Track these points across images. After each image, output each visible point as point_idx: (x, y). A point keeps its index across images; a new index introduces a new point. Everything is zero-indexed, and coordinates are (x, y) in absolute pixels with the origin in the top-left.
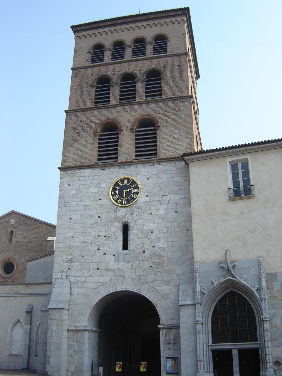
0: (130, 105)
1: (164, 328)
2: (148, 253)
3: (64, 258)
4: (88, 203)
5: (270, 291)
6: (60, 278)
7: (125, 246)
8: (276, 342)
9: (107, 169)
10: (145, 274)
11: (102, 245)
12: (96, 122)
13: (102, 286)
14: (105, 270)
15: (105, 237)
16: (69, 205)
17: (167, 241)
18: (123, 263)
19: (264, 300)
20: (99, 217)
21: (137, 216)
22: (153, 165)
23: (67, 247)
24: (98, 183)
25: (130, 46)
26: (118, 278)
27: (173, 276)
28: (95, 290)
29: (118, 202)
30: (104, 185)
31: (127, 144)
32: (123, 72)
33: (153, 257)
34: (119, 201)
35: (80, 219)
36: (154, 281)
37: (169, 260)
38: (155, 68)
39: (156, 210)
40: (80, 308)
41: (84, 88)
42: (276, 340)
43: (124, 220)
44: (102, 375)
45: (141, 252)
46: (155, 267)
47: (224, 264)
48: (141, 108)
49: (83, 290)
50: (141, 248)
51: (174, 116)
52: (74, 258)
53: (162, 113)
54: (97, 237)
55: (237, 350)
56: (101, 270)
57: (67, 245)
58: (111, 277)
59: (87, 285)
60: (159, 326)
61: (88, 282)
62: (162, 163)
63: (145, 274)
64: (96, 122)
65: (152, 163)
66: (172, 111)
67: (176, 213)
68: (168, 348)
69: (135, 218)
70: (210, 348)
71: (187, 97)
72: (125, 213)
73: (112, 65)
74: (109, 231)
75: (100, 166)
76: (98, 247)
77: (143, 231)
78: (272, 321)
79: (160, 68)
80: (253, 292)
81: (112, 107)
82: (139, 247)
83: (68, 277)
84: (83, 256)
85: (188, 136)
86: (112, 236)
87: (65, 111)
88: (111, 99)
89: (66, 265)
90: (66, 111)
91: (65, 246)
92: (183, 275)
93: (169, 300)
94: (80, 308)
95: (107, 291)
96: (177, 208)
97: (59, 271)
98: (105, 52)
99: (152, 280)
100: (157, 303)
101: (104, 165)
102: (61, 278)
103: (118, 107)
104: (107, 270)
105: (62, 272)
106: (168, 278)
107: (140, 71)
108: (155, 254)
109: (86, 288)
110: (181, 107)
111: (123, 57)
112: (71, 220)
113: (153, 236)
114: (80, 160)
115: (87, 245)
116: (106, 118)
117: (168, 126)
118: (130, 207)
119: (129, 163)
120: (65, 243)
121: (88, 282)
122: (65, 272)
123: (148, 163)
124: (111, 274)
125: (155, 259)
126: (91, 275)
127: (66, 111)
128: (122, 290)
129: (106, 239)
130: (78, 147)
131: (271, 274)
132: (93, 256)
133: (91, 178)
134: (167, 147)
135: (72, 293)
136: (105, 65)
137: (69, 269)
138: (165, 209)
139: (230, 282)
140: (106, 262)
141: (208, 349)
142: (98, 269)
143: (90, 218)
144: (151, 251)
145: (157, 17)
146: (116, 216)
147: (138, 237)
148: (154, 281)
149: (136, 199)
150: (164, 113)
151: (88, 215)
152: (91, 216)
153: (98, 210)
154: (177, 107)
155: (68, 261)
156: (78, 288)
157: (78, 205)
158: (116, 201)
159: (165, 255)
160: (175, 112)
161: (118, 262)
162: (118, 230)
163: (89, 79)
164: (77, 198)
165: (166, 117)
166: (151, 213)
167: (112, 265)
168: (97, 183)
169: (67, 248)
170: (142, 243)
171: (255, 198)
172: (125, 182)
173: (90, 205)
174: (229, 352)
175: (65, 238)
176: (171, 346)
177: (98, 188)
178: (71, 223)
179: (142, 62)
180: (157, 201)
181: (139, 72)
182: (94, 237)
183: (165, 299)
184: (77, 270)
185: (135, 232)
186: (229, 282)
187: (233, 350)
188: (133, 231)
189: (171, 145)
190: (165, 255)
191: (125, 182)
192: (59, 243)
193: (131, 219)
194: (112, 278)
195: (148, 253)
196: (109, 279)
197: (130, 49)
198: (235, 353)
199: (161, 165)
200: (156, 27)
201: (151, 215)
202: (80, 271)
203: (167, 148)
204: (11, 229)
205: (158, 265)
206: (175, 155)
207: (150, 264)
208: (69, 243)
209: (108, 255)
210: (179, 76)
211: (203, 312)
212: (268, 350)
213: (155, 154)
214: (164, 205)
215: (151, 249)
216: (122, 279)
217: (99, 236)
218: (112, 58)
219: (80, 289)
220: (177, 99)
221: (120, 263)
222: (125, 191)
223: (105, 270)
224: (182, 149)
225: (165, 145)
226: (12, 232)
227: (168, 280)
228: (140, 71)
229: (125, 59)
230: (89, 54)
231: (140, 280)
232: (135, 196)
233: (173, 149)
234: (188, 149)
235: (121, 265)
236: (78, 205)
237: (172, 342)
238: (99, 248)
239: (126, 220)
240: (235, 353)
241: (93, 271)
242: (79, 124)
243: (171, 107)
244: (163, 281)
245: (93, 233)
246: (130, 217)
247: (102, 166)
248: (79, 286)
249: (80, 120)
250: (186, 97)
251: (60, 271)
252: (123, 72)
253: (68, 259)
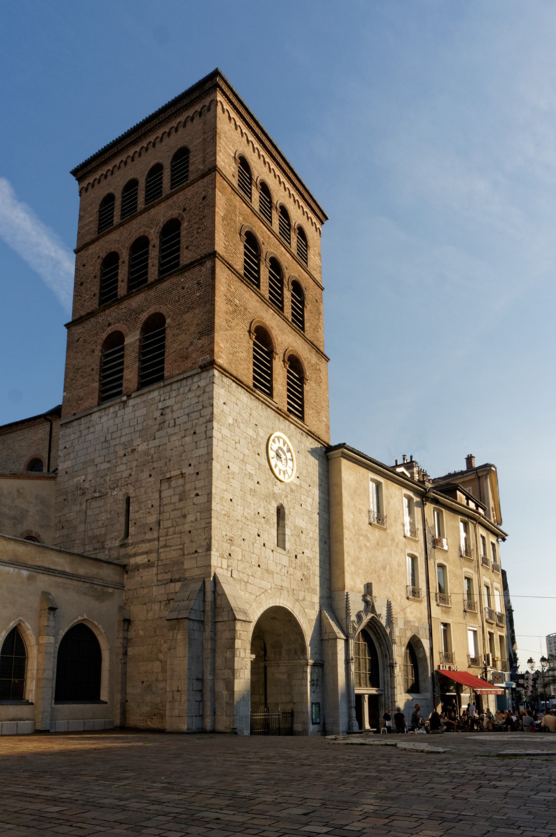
3: (224, 533)
16: (226, 442)
91: (223, 512)
102: (221, 568)
169: (226, 518)
178: (230, 476)
236: (236, 448)
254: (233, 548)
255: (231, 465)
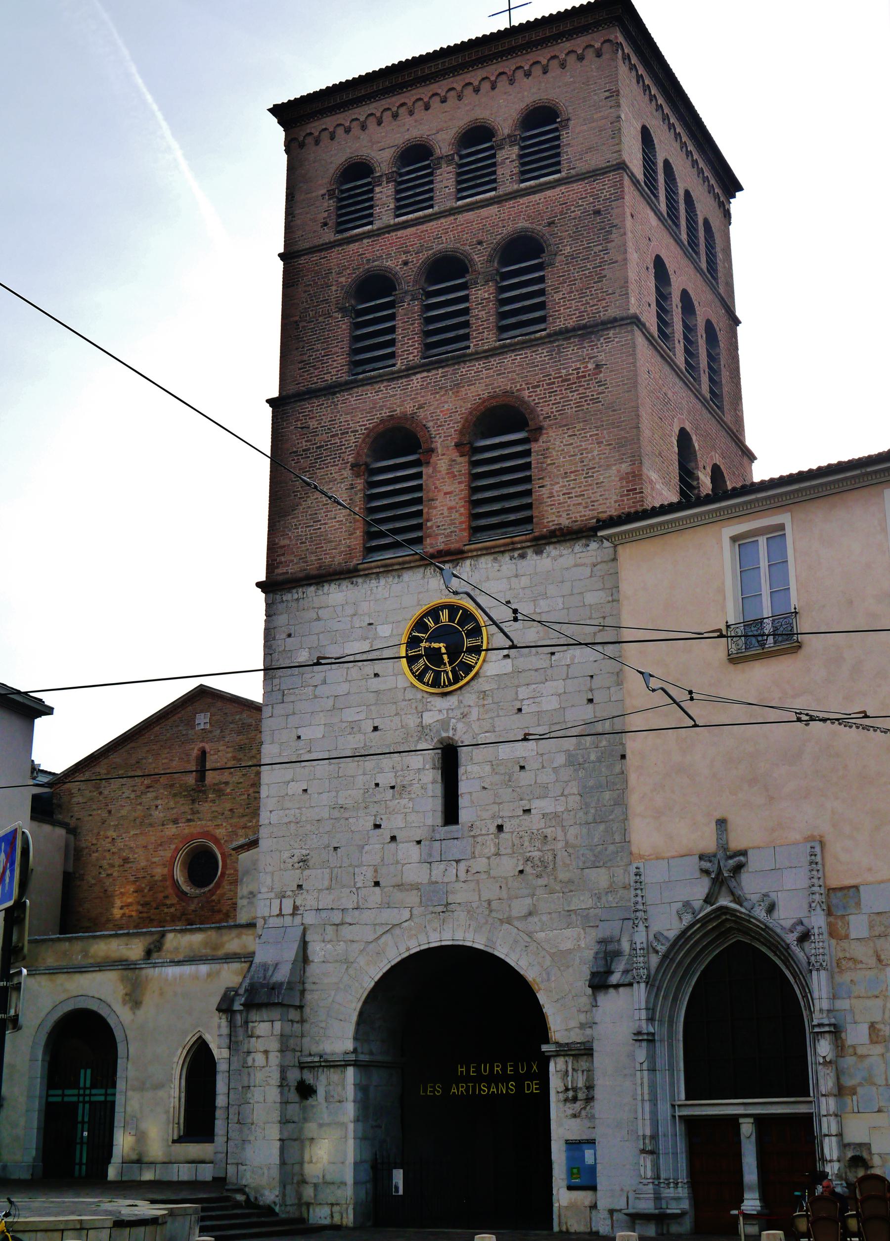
0: (454, 364)
1: (557, 1054)
2: (512, 833)
3: (286, 855)
4: (344, 688)
5: (840, 942)
6: (278, 915)
7: (451, 815)
8: (855, 1098)
9: (394, 577)
10: (504, 894)
11: (386, 813)
12: (357, 431)
13: (388, 935)
14: (394, 886)
15: (393, 787)
16: (292, 698)
17: (565, 793)
18: (442, 866)
19: (818, 970)
20: (376, 729)
21: (479, 719)
22: (523, 556)
23: (292, 824)
24: (370, 624)
25: (449, 159)
26: (431, 909)
27: (582, 898)
28: (372, 946)
29: (426, 680)
30: (384, 630)
31: (446, 494)
32: (430, 252)
33: (526, 844)
34: (430, 676)
35: (324, 736)
36: (530, 914)
37: (570, 850)
38: (526, 230)
39: (532, 701)
40: (330, 1000)
41: (321, 319)
42: (855, 1093)
43: (444, 735)
44: (401, 1192)
45: (493, 829)
46: (532, 874)
47: (710, 861)
48: (484, 372)
49: (338, 948)
50: (493, 817)
51: (581, 390)
52: (311, 853)
53: (548, 384)
54: (371, 790)
55: (751, 1120)
56: (385, 887)
57: (292, 818)
58: (412, 908)
59: (346, 931)
60: (544, 1048)
61: (350, 924)
62: (550, 548)
63: (504, 894)
64: (358, 428)
65: (520, 552)
66: (578, 373)
67: (590, 706)
68: (570, 1112)
69: (473, 726)
70: (677, 1114)
71: (622, 323)
72: (445, 712)
73: (399, 233)
74: (402, 770)
75: (370, 572)
76: (375, 820)
77: (498, 765)
78: (843, 1035)
79: (540, 228)
80: (788, 945)
81: (401, 377)
82: (486, 815)
83: (299, 912)
84: (335, 849)
85: (624, 454)
86: (411, 785)
87: (268, 401)
88: (398, 349)
89: (291, 878)
90: (270, 402)
91: (286, 820)
92: (609, 895)
93: (571, 970)
94: (333, 1001)
95: (402, 949)
96: (591, 690)
97: (272, 895)
98: (377, 189)
99: (524, 912)
100: (538, 980)
101: (383, 566)
102: (280, 915)
103: (419, 376)
104: (400, 886)
105: (282, 896)
106: (569, 906)
107: (480, 243)
108: (533, 833)
109: (344, 941)
110: (602, 357)
111: (429, 202)
112: (301, 743)
113: (525, 778)
114: (316, 556)
115: (347, 815)
116: (385, 413)
117: (565, 426)
118: (459, 692)
119: (455, 556)
120: (287, 812)
121: (350, 924)
122: (289, 896)
123: (509, 550)
124: (413, 898)
125: (532, 849)
126: (358, 902)
127: (270, 402)
128: (444, 943)
129: (397, 796)
130: (310, 515)
131: (841, 889)
132: (363, 848)
133: (349, 610)
134: (564, 494)
135: (311, 959)
136: (378, 235)
137: (300, 887)
138: (559, 695)
139: (728, 917)
140: (398, 862)
141: (674, 1117)
142: (377, 884)
143: (350, 734)
144: (519, 826)
145: (527, 43)
146: (422, 722)
147: (483, 785)
148: (530, 914)
149: (474, 667)
150: (554, 383)
151: (345, 725)
152: (354, 727)
153: (373, 708)
154: (591, 358)
155: (297, 865)
156: (324, 941)
157: (316, 697)
158: (420, 677)
159: (560, 835)
160: (584, 376)
161: (430, 863)
162: (427, 767)
163: (334, 288)
164: (313, 674)
165: (558, 397)
166: (520, 710)
167: (416, 873)
168: (366, 624)
170: (494, 803)
171: (802, 653)
172: (444, 616)
173: (348, 693)
174: (733, 1122)
175: (287, 798)
176: (578, 1105)
177: (368, 641)
179: (484, 212)
180: (536, 670)
181: (479, 247)
182: (362, 791)
183: (562, 968)
184: (322, 890)
185: (476, 768)
186: (724, 917)
187: (741, 1120)
188: (469, 767)
189: (574, 488)
190: (560, 835)
191: (444, 616)
192: (271, 812)
193: (464, 730)
194: (415, 912)
195: (512, 833)
196: (406, 914)
197: (450, 168)
198: (747, 1128)
199: (545, 555)
200: (525, 80)
201: (519, 715)
202: (327, 892)
203: (561, 497)
204: (201, 745)
205: (544, 867)
206: (586, 520)
207: (517, 865)
208: (297, 811)
209: (403, 842)
210: (596, 249)
211: (655, 1005)
212: (829, 1123)
213: (529, 520)
214: (555, 683)
215: (521, 818)
216: (443, 912)
217: (377, 785)
218: (398, 208)
219: (329, 946)
220: (592, 333)
221: (434, 865)
222: (441, 645)
223: (394, 886)
224: (606, 499)
225: (557, 488)
226: (203, 753)
227: (568, 911)
228: (480, 243)
229: (436, 209)
230: (329, 199)
231: (491, 911)
232: (470, 659)
233: (580, 500)
234: (625, 498)
235: (438, 870)
236: (316, 697)
237: (581, 1095)
238: (378, 823)
239: (451, 734)
240: (747, 1128)
241: (363, 892)
242: (311, 441)
243: (573, 362)
244: (554, 915)
245: (360, 780)
246: (460, 726)
247: (378, 570)
248: (328, 938)
249: (311, 427)
250: (616, 324)
251: (276, 895)
252: (430, 252)
253: (296, 859)
254: (306, 872)
255: (300, 732)
